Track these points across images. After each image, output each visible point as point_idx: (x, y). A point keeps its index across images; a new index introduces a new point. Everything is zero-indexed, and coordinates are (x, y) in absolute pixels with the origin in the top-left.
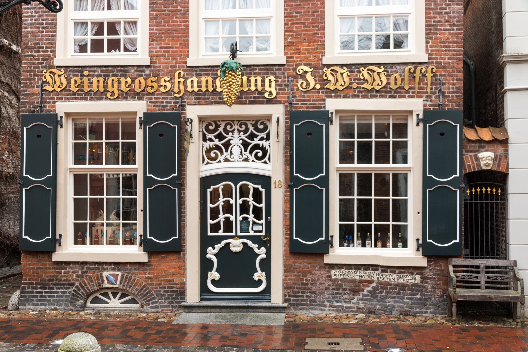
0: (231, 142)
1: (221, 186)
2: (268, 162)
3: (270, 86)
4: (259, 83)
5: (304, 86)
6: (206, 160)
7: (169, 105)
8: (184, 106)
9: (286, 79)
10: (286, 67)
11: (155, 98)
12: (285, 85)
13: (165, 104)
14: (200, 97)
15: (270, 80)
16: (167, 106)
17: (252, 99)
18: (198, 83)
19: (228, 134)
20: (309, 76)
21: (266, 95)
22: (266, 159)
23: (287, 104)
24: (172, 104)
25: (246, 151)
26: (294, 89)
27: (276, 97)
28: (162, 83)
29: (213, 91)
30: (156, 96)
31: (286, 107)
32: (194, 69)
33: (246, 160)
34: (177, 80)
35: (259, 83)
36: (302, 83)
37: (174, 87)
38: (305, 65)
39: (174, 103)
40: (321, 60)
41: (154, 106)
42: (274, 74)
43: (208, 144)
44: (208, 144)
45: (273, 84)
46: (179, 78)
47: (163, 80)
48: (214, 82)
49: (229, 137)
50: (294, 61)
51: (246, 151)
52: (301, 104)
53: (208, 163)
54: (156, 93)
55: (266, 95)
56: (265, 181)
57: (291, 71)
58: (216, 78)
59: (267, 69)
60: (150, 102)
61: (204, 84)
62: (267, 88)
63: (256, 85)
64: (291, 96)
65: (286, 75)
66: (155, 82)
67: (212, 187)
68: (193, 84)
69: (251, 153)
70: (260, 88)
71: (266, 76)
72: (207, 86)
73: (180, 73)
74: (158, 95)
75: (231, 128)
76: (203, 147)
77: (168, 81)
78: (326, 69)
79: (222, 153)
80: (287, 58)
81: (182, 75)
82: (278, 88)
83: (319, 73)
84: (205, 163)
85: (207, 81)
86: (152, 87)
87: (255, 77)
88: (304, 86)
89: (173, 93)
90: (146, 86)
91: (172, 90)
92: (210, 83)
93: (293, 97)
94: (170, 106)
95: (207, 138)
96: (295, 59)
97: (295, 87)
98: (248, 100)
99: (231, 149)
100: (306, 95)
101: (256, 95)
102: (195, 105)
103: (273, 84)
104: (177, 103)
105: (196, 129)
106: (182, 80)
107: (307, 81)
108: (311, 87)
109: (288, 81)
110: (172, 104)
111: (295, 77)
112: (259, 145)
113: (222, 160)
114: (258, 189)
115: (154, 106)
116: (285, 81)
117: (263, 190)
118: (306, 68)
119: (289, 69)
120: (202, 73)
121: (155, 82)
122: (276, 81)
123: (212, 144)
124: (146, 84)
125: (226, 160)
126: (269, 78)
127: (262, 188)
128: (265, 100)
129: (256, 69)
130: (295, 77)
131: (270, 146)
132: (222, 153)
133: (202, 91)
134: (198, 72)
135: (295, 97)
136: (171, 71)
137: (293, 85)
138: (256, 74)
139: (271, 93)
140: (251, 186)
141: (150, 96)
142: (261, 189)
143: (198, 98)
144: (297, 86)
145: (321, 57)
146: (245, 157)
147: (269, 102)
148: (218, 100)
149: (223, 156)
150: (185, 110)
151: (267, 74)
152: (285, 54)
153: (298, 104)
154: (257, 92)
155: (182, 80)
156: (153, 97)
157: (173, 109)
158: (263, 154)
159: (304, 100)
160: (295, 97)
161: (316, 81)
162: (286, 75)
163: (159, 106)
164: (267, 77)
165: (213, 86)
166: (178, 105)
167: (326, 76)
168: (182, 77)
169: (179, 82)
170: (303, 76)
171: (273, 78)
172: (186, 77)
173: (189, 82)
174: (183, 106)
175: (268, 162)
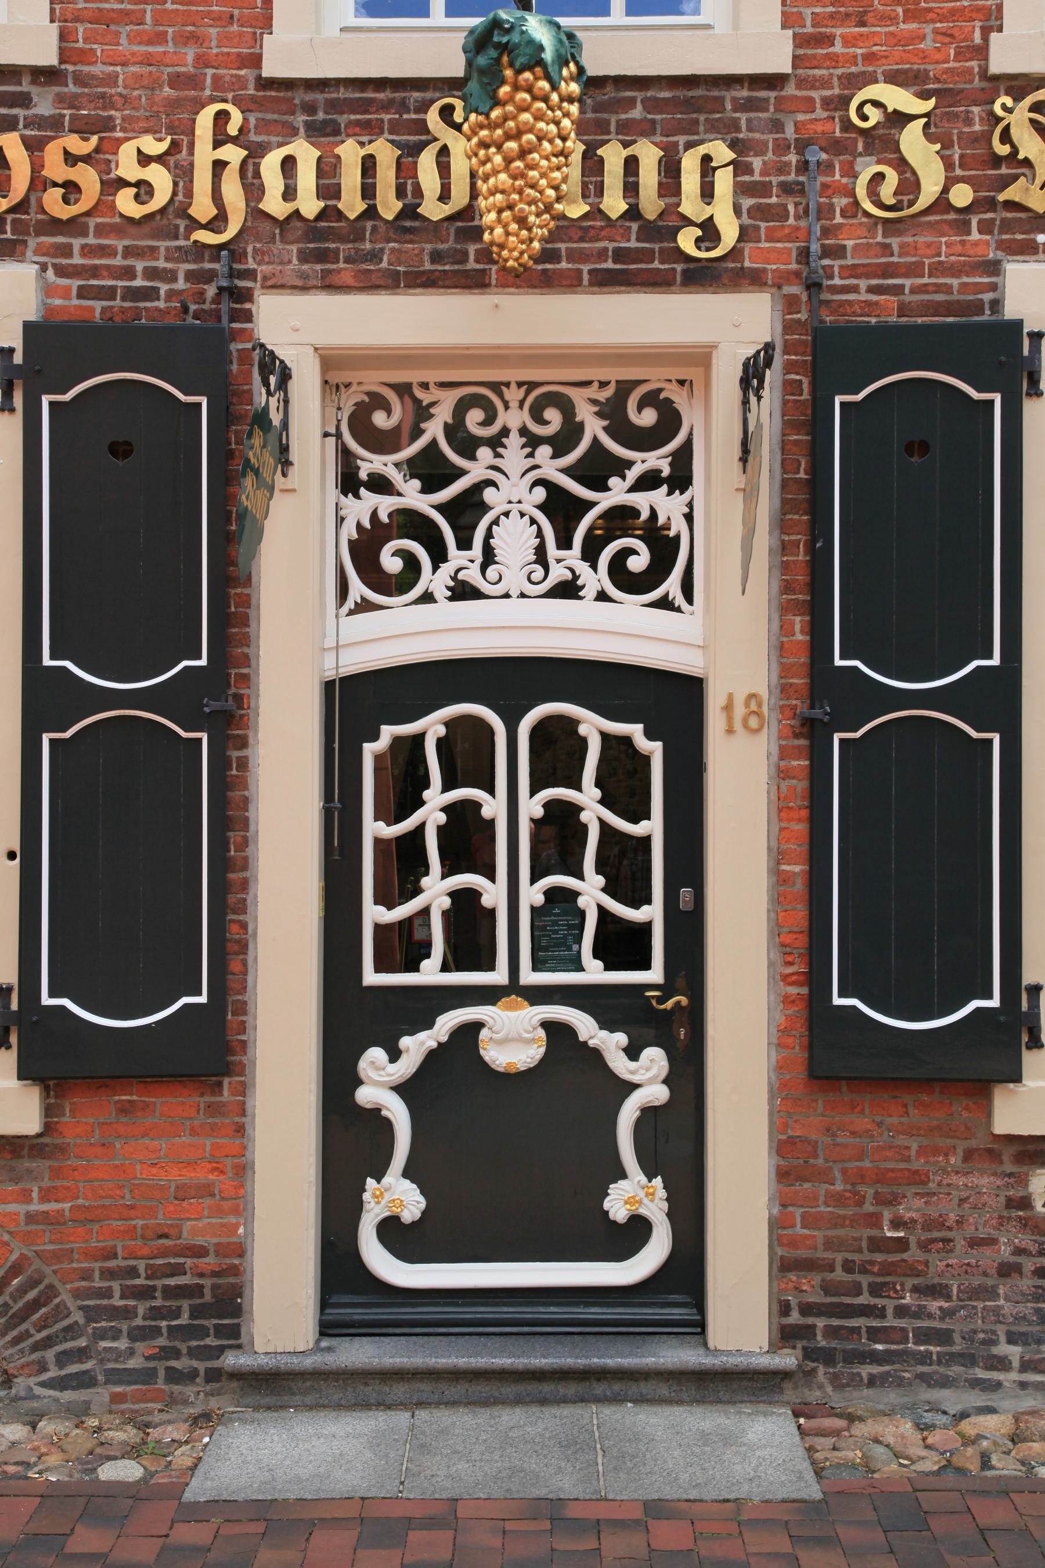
0: (489, 495)
1: (432, 726)
2: (680, 601)
3: (707, 193)
4: (649, 177)
5: (887, 192)
6: (358, 588)
7: (164, 288)
8: (246, 296)
9: (793, 158)
10: (791, 90)
11: (87, 251)
12: (786, 189)
13: (139, 282)
14: (334, 249)
15: (706, 159)
16: (150, 294)
17: (609, 265)
18: (320, 173)
19: (472, 457)
20: (912, 141)
21: (686, 241)
22: (672, 585)
23: (795, 289)
24: (181, 284)
25: (564, 542)
26: (831, 208)
27: (734, 253)
28: (127, 167)
29: (401, 215)
30: (91, 240)
31: (791, 304)
32: (300, 96)
33: (568, 590)
34: (204, 154)
35: (649, 177)
36: (880, 177)
37: (189, 194)
38: (894, 78)
39: (190, 276)
40: (982, 52)
41: (83, 293)
42: (726, 130)
43: (363, 507)
44: (363, 507)
45: (724, 181)
46: (217, 144)
47: (127, 153)
48: (406, 170)
49: (476, 471)
50: (834, 60)
51: (564, 542)
52: (871, 290)
53: (364, 606)
54: (92, 222)
55: (686, 241)
56: (672, 701)
57: (820, 113)
58: (417, 149)
59: (689, 102)
60: (61, 271)
61: (351, 179)
62: (690, 205)
63: (631, 189)
64: (815, 247)
65: (790, 132)
66: (86, 159)
67: (388, 732)
68: (293, 177)
69: (590, 555)
70: (651, 204)
71: (682, 140)
72: (368, 191)
73: (222, 117)
74: (100, 231)
75: (490, 420)
76: (340, 520)
77: (160, 159)
78: (1009, 102)
79: (439, 557)
80: (800, 41)
81: (233, 129)
82: (747, 203)
83: (969, 121)
84: (350, 604)
85: (369, 165)
86: (71, 189)
87: (626, 145)
88: (887, 192)
89: (182, 224)
90: (39, 182)
91: (179, 207)
92: (386, 176)
93: (827, 252)
94: (171, 294)
95: (363, 475)
96: (838, 48)
97: (841, 202)
98: (585, 268)
99: (489, 535)
100: (895, 242)
101: (633, 244)
102: (304, 289)
103: (724, 181)
104: (209, 277)
105: (308, 418)
106: (233, 154)
107: (902, 164)
108: (925, 200)
109: (804, 167)
110: (181, 284)
111: (835, 147)
112: (635, 512)
113: (441, 592)
114: (627, 741)
115: (83, 293)
116: (782, 168)
117: (654, 749)
118: (899, 98)
119: (809, 105)
120: (343, 119)
121: (86, 159)
122: (739, 167)
123: (386, 505)
124: (36, 168)
125: (463, 591)
126: (702, 150)
127: (650, 735)
128: (679, 267)
129: (631, 103)
130: (835, 147)
131: (689, 518)
132: (439, 557)
133: (340, 215)
134: (321, 116)
135: (838, 252)
136: (173, 105)
137: (825, 186)
138: (629, 132)
139: (709, 232)
140: (592, 725)
141: (60, 239)
142: (643, 744)
143: (322, 256)
144: (853, 195)
145: (977, 38)
146: (558, 573)
147: (700, 276)
148: (428, 266)
149: (446, 569)
150: (248, 316)
151: (691, 127)
152: (787, 21)
153: (855, 289)
154: (635, 226)
155: (233, 154)
156: (77, 243)
157: (185, 310)
158: (656, 566)
159: (887, 271)
160: (838, 252)
161: (949, 166)
162: (790, 132)
163: (109, 293)
164: (689, 146)
165: (400, 193)
166: (211, 291)
167: (1006, 137)
168: (234, 140)
169: (219, 166)
170: (883, 139)
171: (721, 152)
172: (253, 137)
173: (270, 165)
174: (238, 298)
175: (680, 601)
